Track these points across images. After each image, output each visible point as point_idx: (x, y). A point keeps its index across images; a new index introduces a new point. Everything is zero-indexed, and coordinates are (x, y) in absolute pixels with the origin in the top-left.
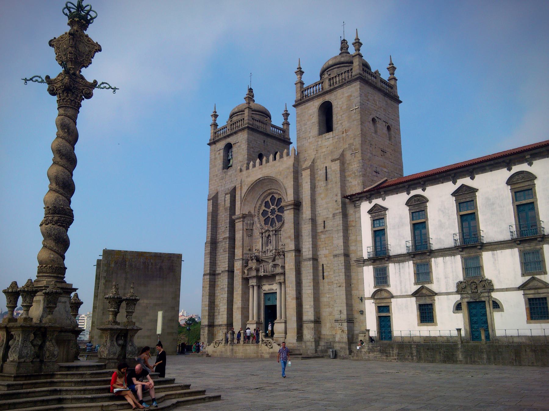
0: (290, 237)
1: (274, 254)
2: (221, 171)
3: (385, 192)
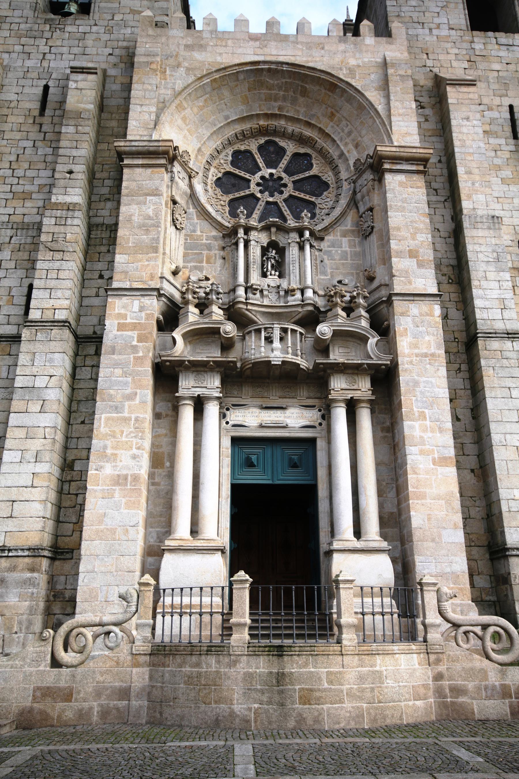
0: (412, 254)
1: (312, 302)
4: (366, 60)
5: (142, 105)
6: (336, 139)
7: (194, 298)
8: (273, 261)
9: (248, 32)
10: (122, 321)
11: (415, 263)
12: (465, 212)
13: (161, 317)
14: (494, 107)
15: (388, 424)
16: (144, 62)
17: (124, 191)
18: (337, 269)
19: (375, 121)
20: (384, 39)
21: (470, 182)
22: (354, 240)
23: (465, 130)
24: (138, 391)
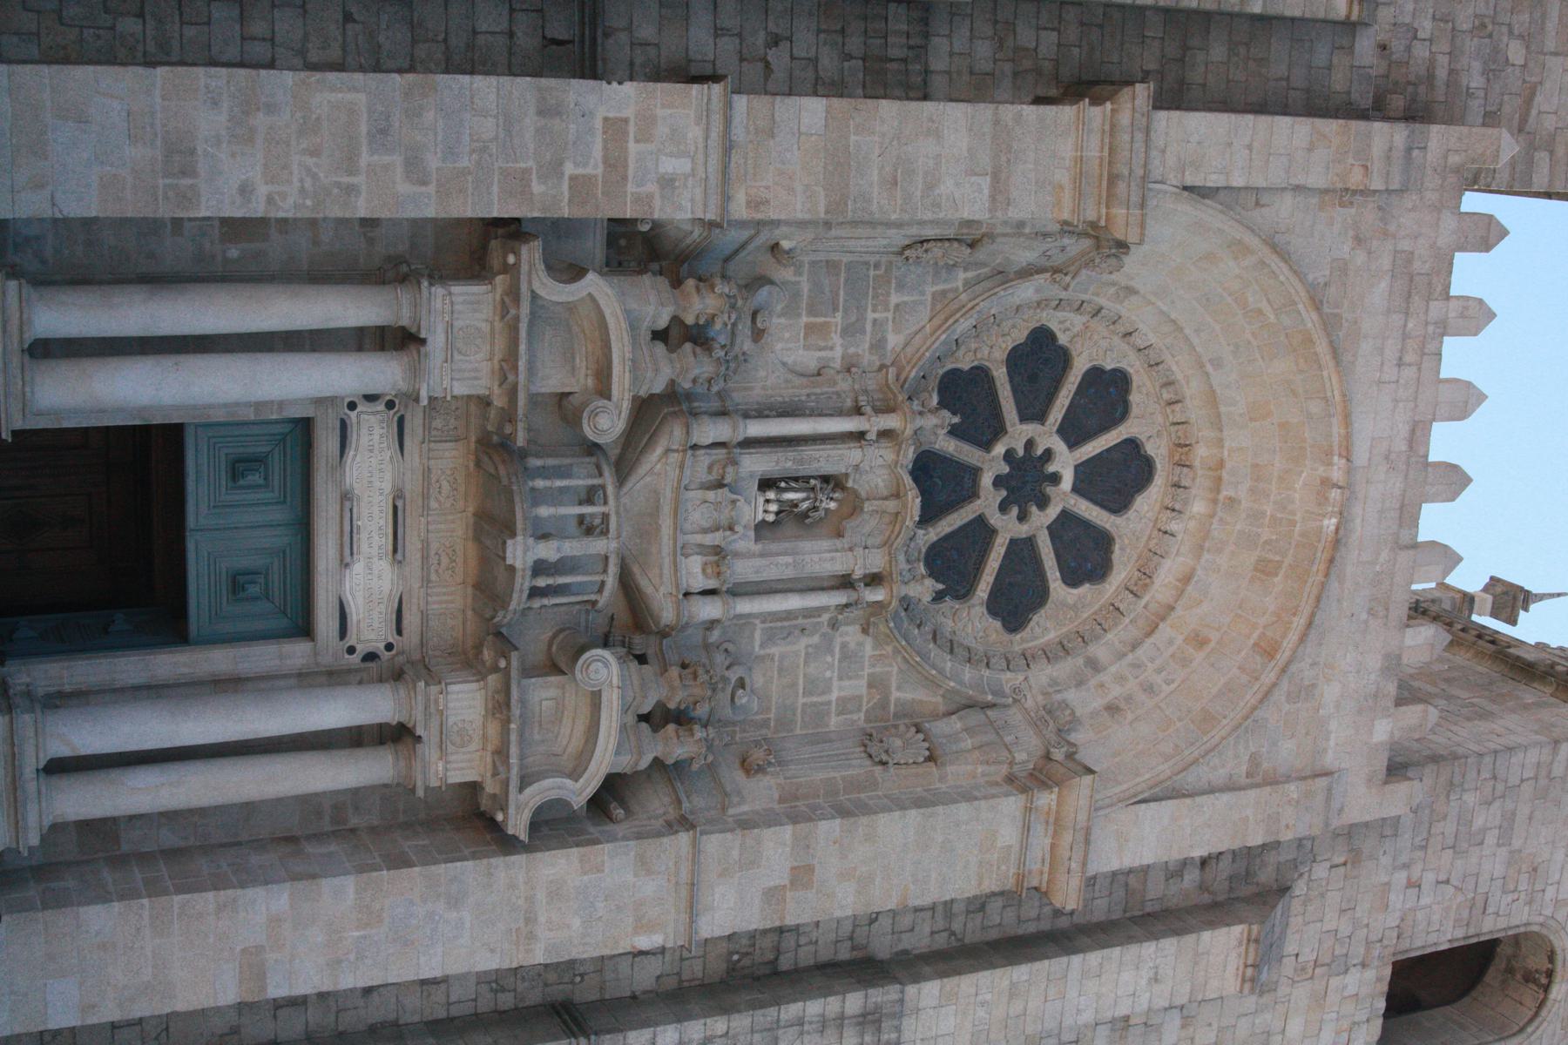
0: (802, 875)
4: (1333, 725)
5: (1250, 147)
6: (1139, 652)
7: (698, 317)
8: (805, 505)
9: (1434, 420)
10: (632, 129)
11: (778, 882)
12: (911, 990)
13: (645, 228)
14: (1191, 1029)
15: (354, 821)
16: (1369, 146)
17: (1008, 112)
18: (780, 670)
19: (1167, 758)
20: (1381, 763)
21: (988, 997)
22: (859, 710)
23: (1126, 976)
24: (431, 189)
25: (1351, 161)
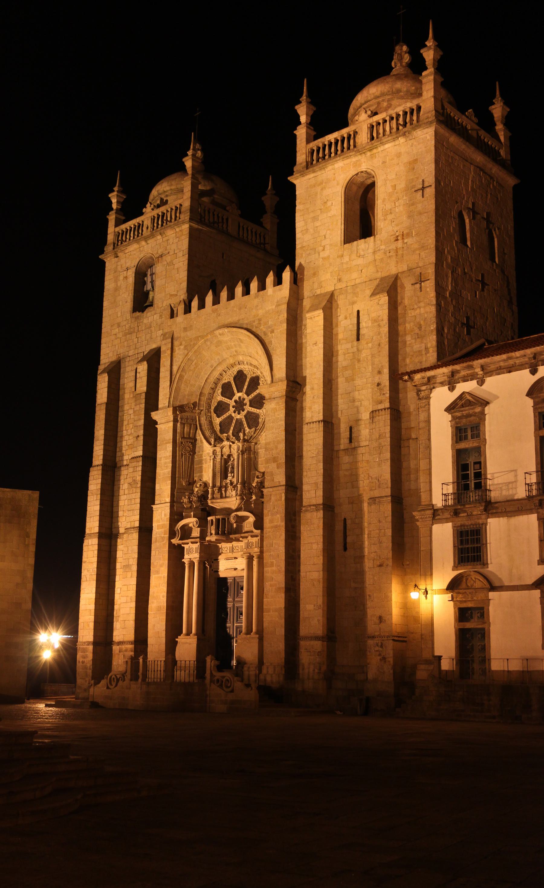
0: (275, 460)
2: (128, 316)
3: (483, 368)
4: (267, 309)
21: (312, 396)
25: (166, 354)
